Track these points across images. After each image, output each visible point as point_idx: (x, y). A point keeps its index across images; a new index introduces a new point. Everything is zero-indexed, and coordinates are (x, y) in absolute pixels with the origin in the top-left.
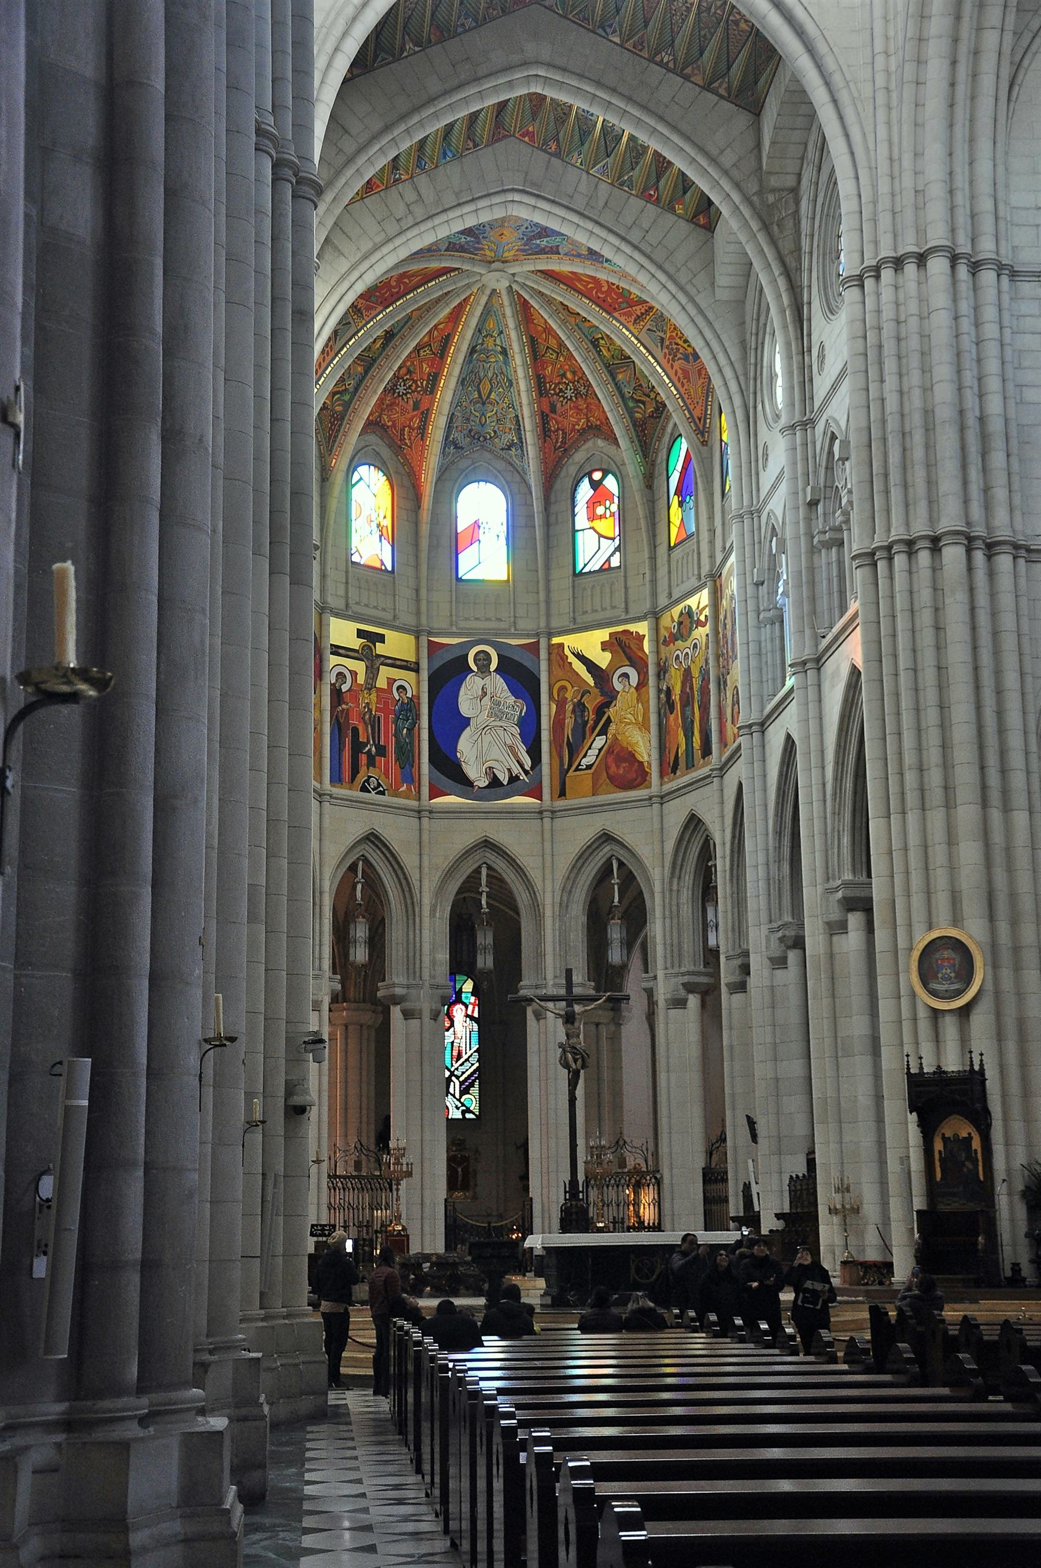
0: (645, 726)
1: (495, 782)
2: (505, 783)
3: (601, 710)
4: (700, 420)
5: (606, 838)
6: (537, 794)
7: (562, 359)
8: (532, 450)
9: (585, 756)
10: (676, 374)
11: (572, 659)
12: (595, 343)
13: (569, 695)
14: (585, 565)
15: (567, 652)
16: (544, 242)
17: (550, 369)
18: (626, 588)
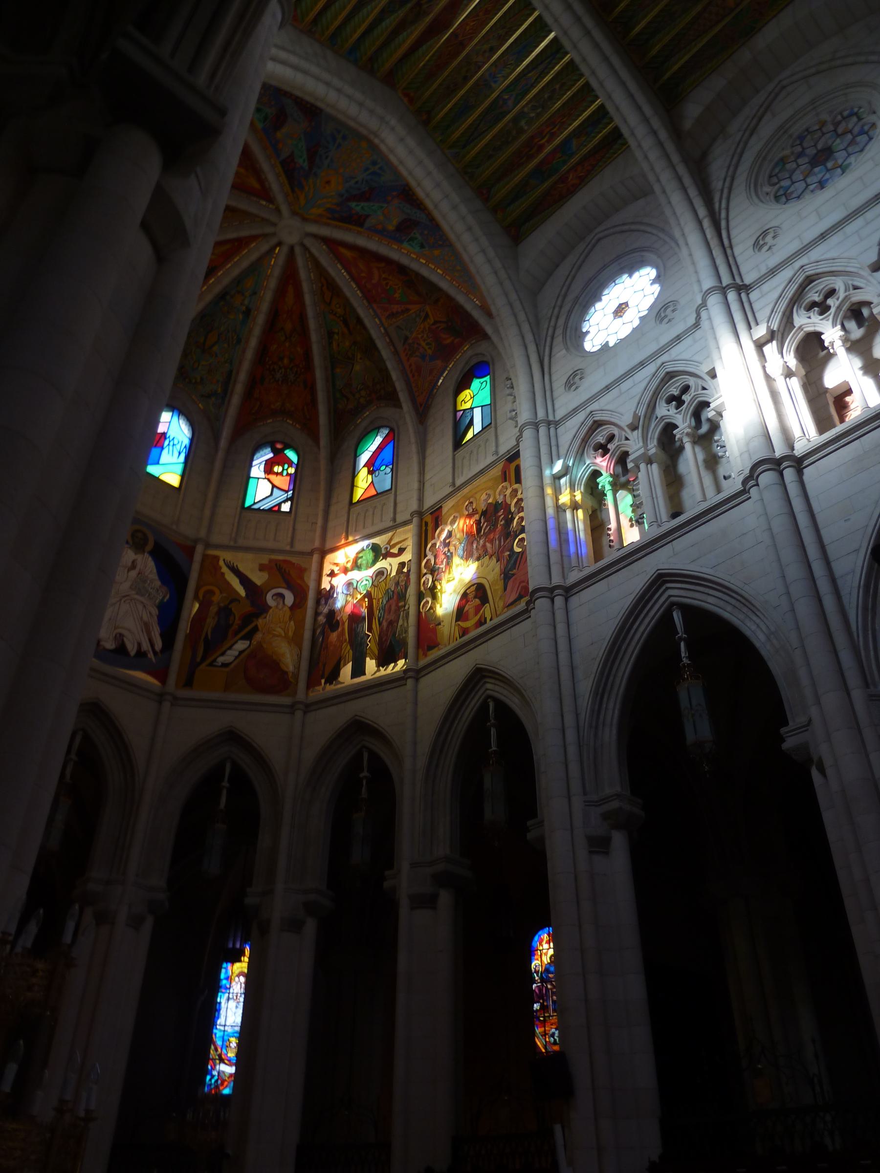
0: (296, 640)
1: (121, 649)
2: (133, 653)
3: (248, 618)
4: (421, 405)
5: (232, 737)
6: (162, 675)
7: (287, 344)
8: (236, 400)
9: (223, 654)
10: (410, 365)
11: (225, 569)
12: (330, 334)
13: (216, 598)
14: (255, 503)
15: (221, 563)
16: (357, 207)
17: (275, 346)
18: (294, 529)
